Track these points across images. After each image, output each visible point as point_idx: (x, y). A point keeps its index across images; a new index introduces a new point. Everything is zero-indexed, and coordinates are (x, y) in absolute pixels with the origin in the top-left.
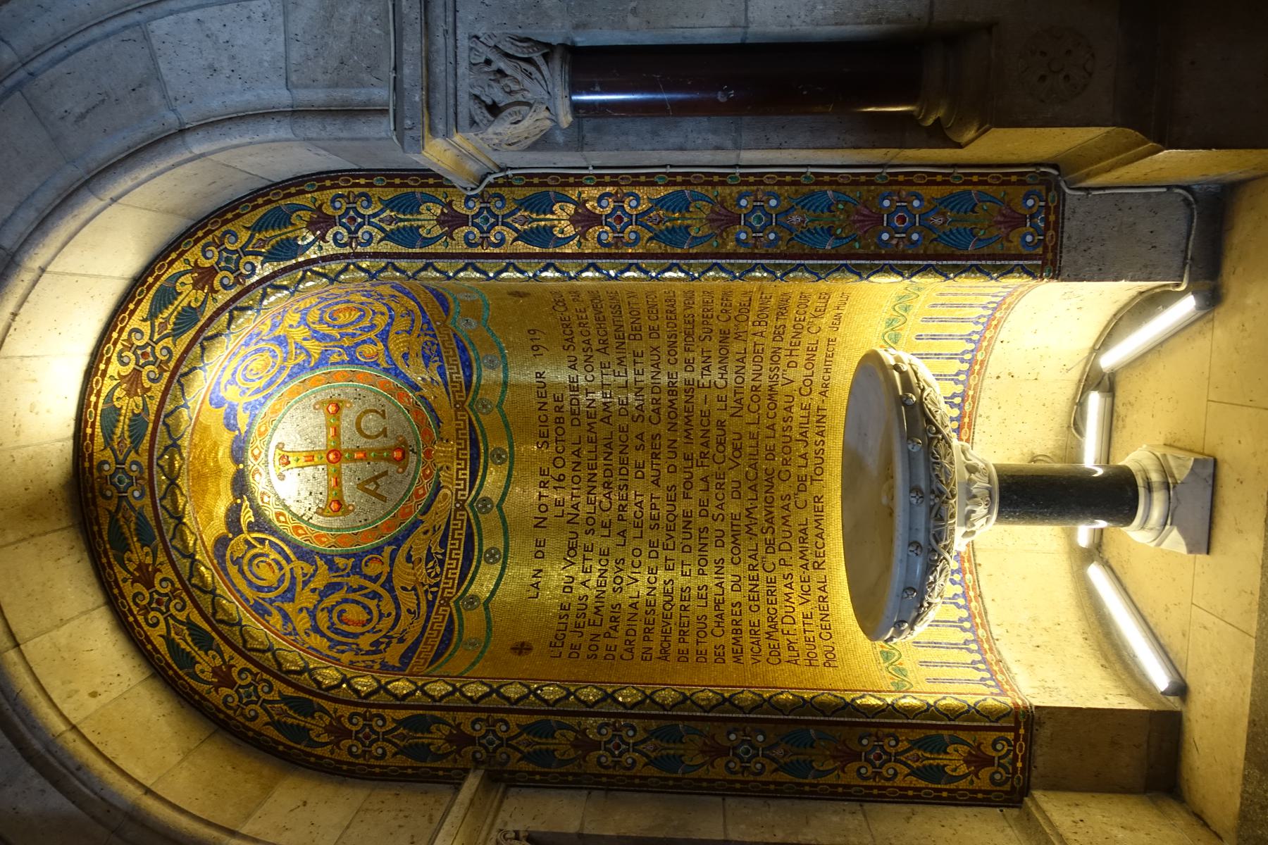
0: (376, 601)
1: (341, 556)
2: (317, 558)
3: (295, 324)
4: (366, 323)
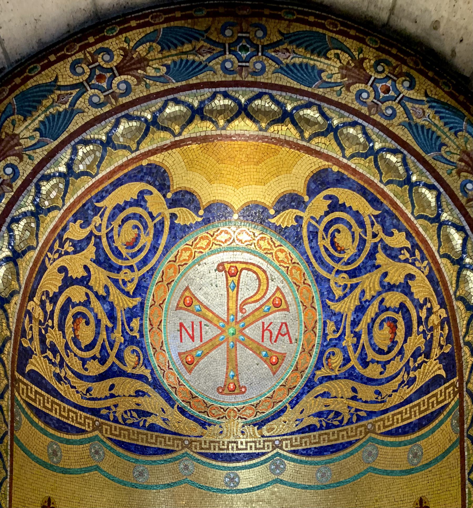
0: (98, 355)
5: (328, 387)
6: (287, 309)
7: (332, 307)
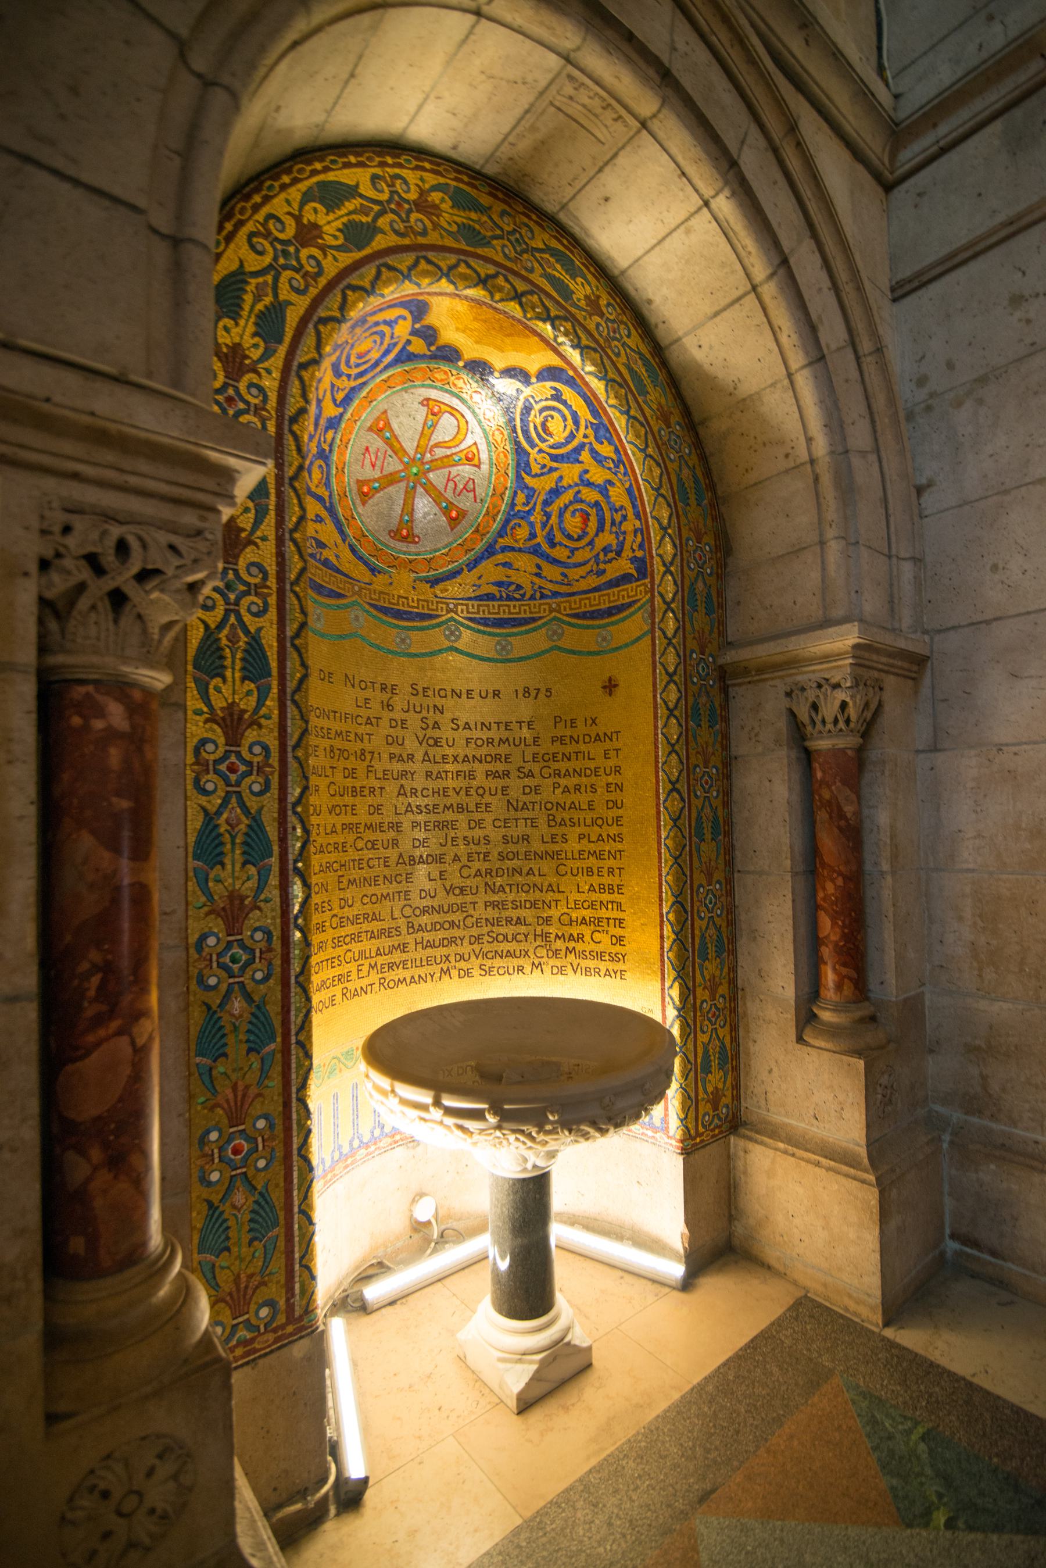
1: (333, 439)
2: (341, 410)
3: (587, 476)
4: (559, 537)
5: (510, 558)
6: (478, 467)
7: (526, 481)
